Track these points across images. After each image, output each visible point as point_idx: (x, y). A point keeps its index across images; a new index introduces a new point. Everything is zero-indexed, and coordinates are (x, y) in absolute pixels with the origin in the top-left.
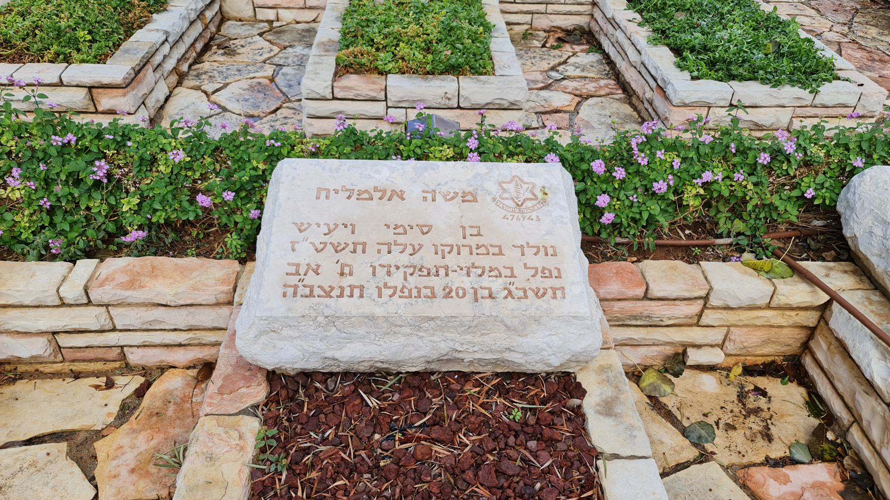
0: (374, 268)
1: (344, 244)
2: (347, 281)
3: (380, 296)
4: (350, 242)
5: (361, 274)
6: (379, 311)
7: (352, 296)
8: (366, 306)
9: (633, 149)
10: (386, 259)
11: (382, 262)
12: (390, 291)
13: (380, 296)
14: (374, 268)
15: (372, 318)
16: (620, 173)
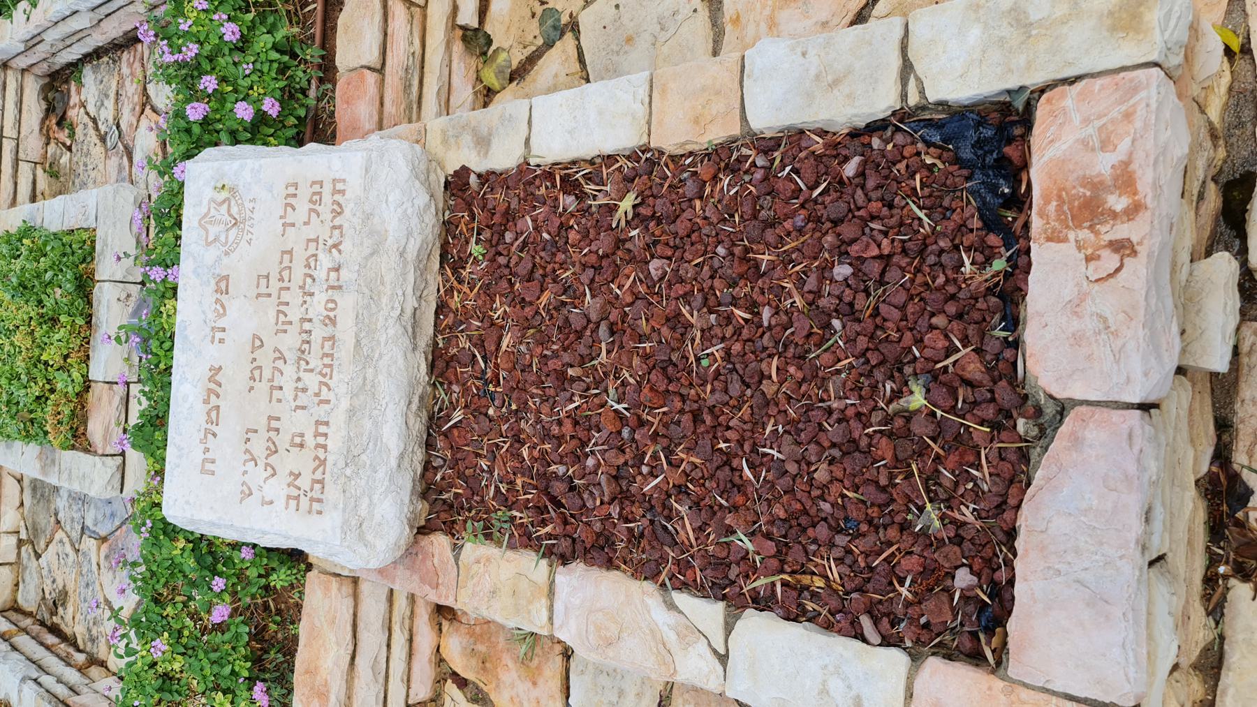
0: (297, 407)
1: (267, 442)
2: (310, 441)
3: (328, 402)
4: (267, 435)
5: (301, 423)
6: (345, 404)
7: (326, 435)
8: (338, 418)
9: (176, 61)
10: (288, 392)
11: (291, 398)
12: (324, 389)
13: (328, 402)
14: (297, 407)
15: (352, 412)
16: (209, 83)
